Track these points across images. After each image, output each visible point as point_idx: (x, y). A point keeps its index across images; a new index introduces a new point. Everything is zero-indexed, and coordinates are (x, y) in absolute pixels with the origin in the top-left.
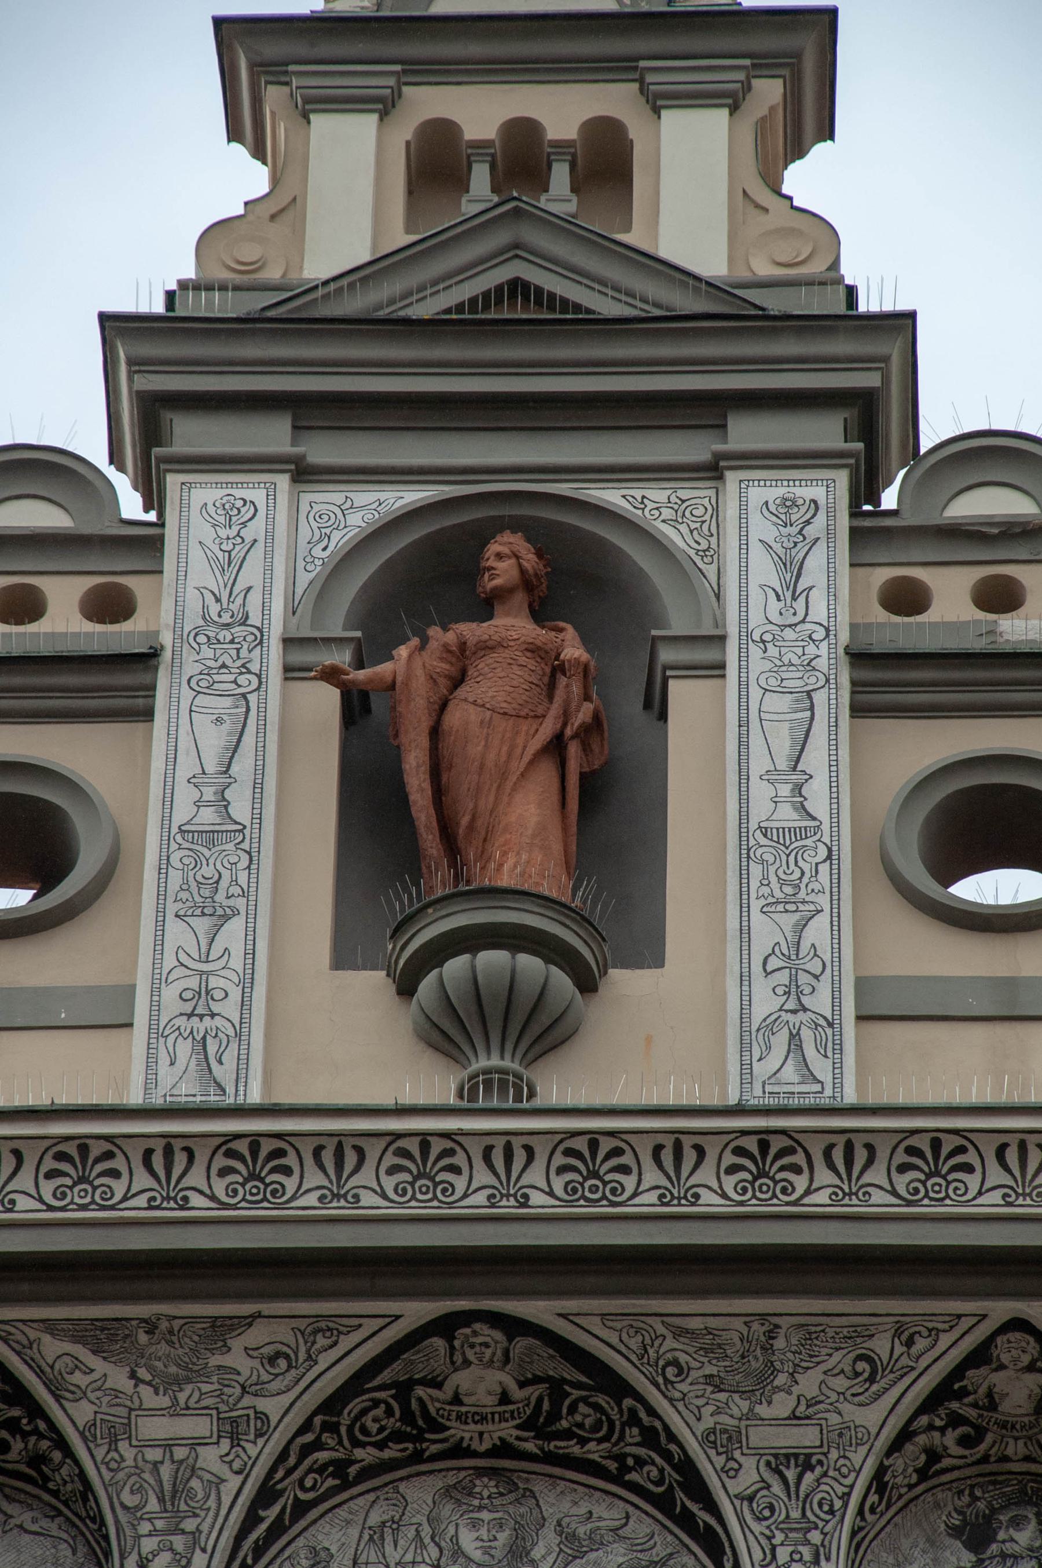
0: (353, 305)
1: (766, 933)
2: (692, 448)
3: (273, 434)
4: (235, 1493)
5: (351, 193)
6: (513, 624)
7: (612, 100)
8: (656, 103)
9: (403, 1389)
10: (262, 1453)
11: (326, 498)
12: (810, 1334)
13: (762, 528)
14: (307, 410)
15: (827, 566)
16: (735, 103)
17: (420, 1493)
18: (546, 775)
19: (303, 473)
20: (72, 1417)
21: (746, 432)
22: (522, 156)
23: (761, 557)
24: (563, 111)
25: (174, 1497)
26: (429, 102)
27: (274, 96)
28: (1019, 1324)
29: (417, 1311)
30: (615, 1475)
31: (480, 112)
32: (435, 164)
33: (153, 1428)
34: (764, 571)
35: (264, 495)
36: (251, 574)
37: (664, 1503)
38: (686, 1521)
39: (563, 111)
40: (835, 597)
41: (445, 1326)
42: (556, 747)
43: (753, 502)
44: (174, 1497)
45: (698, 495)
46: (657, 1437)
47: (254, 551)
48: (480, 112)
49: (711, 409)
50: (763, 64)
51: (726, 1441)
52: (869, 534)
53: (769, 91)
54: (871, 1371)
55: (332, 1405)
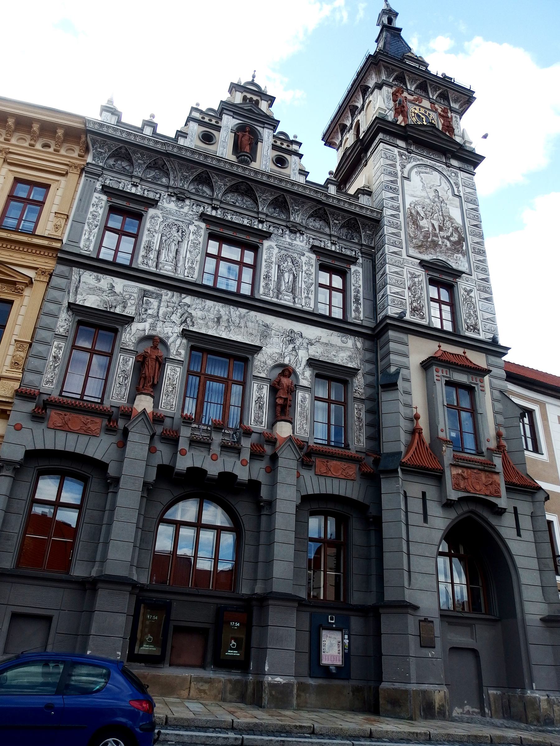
0: (240, 106)
1: (264, 162)
2: (262, 126)
3: (232, 114)
5: (238, 98)
6: (247, 134)
7: (259, 98)
8: (262, 100)
9: (237, 186)
10: (226, 187)
11: (235, 120)
12: (268, 191)
13: (267, 133)
14: (234, 112)
15: (271, 137)
16: (267, 101)
17: (236, 194)
18: (249, 146)
19: (233, 117)
20: (213, 180)
21: (266, 125)
22: (251, 99)
23: (267, 135)
24: (255, 98)
26: (245, 94)
27: (234, 89)
28: (283, 195)
29: (241, 180)
30: (250, 197)
31: (249, 96)
32: (245, 98)
33: (219, 183)
34: (266, 136)
35: (231, 118)
36: (229, 123)
37: (254, 200)
38: (255, 202)
39: (255, 98)
40: (271, 140)
41: (242, 182)
42: (250, 144)
43: (266, 130)
45: (262, 129)
46: (255, 195)
47: (229, 122)
48: (249, 96)
49: (264, 123)
50: (270, 100)
51: (260, 197)
52: (274, 136)
53: (270, 102)
54: (271, 195)
55: (232, 185)
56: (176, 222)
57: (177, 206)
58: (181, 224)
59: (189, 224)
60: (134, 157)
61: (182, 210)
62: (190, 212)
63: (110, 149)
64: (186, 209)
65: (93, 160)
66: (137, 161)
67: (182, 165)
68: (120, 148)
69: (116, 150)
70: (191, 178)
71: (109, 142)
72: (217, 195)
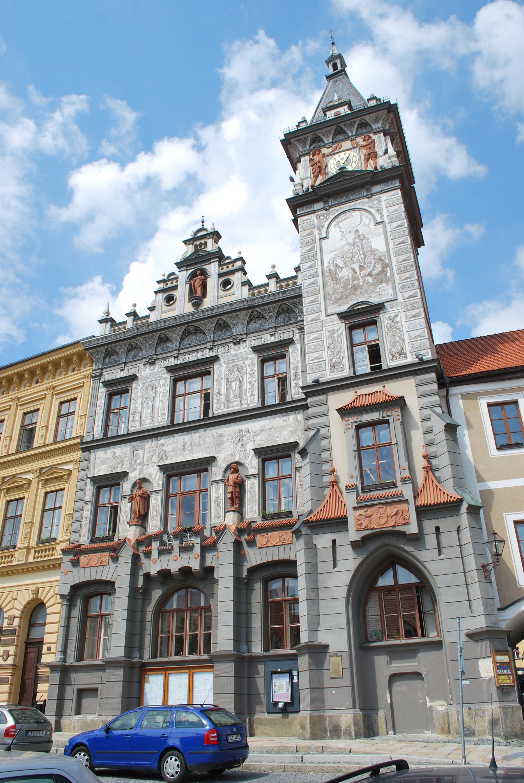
4: (179, 339)
20: (169, 336)
25: (176, 340)
44: (176, 340)
56: (151, 383)
57: (150, 370)
58: (153, 383)
59: (160, 379)
60: (117, 350)
61: (154, 371)
62: (160, 370)
63: (102, 353)
64: (156, 370)
65: (96, 366)
66: (120, 351)
67: (145, 338)
68: (107, 349)
69: (106, 351)
70: (155, 343)
71: (99, 349)
72: (176, 345)
